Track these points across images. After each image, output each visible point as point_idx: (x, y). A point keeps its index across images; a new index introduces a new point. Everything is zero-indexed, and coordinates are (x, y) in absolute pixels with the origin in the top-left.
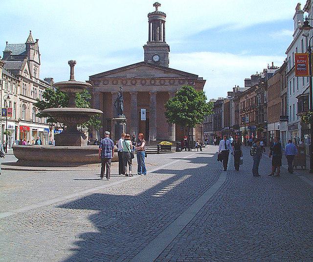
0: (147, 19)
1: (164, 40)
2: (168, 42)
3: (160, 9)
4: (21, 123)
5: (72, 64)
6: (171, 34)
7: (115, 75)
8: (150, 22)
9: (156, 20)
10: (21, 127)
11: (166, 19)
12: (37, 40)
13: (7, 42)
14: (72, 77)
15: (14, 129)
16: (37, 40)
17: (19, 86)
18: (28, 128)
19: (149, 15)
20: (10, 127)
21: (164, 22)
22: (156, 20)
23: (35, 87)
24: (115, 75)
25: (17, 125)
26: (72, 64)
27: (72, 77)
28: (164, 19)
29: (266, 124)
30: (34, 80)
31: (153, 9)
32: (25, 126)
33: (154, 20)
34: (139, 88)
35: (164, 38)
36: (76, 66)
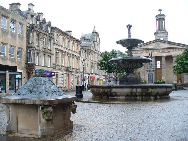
0: (155, 19)
1: (165, 29)
2: (167, 30)
3: (162, 13)
4: (91, 75)
5: (129, 27)
6: (168, 26)
8: (157, 20)
9: (161, 19)
10: (91, 77)
11: (166, 18)
12: (98, 31)
14: (130, 36)
15: (87, 78)
16: (98, 31)
18: (95, 77)
19: (157, 16)
20: (85, 77)
21: (164, 19)
22: (161, 19)
23: (98, 56)
25: (89, 76)
26: (129, 27)
27: (130, 36)
28: (164, 18)
30: (97, 52)
31: (158, 13)
32: (93, 77)
33: (160, 19)
35: (165, 28)
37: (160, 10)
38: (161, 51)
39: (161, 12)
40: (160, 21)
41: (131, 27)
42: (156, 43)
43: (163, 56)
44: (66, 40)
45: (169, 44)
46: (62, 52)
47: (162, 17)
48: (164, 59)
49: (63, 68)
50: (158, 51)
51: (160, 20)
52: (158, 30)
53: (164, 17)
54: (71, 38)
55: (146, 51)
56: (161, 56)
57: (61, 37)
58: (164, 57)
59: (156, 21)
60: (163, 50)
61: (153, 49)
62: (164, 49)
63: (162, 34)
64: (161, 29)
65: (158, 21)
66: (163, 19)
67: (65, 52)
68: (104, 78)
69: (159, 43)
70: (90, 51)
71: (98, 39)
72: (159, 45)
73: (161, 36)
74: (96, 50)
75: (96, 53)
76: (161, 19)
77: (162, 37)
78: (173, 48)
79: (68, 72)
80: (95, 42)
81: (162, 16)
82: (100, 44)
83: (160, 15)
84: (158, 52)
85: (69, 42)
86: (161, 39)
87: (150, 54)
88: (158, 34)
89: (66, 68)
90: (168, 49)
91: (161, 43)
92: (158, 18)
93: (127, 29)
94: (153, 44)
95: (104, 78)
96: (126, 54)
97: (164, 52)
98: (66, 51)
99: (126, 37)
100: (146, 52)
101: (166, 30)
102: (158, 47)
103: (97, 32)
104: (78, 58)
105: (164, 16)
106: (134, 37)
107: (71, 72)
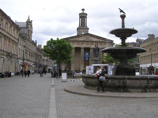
0: (79, 16)
1: (86, 26)
3: (85, 12)
4: (25, 61)
6: (89, 22)
7: (74, 39)
8: (80, 17)
9: (83, 17)
10: (25, 63)
11: (87, 16)
12: (32, 21)
13: (16, 21)
16: (32, 21)
17: (25, 42)
18: (27, 63)
19: (80, 14)
21: (86, 17)
22: (83, 17)
23: (30, 44)
24: (74, 39)
29: (139, 65)
30: (30, 39)
31: (82, 12)
32: (26, 63)
33: (83, 17)
34: (85, 45)
35: (86, 25)
37: (83, 10)
38: (90, 43)
40: (83, 19)
43: (91, 48)
44: (9, 25)
45: (97, 38)
46: (5, 37)
47: (85, 15)
48: (92, 51)
49: (5, 53)
50: (87, 43)
51: (83, 17)
54: (12, 24)
56: (80, 47)
57: (5, 21)
58: (92, 48)
60: (92, 43)
61: (84, 41)
62: (93, 42)
63: (84, 29)
64: (83, 25)
67: (8, 37)
68: (33, 64)
69: (88, 36)
70: (25, 38)
71: (31, 28)
73: (83, 31)
74: (29, 38)
75: (29, 41)
76: (84, 17)
77: (84, 32)
78: (100, 42)
79: (9, 57)
80: (29, 31)
82: (32, 33)
83: (83, 13)
84: (87, 44)
85: (11, 27)
86: (83, 33)
87: (96, 46)
88: (80, 29)
89: (7, 53)
90: (95, 42)
91: (90, 36)
92: (81, 16)
93: (121, 19)
94: (83, 37)
95: (33, 64)
96: (121, 44)
97: (92, 44)
98: (8, 35)
99: (120, 27)
100: (77, 43)
103: (31, 21)
104: (17, 44)
105: (86, 14)
106: (128, 26)
107: (11, 57)
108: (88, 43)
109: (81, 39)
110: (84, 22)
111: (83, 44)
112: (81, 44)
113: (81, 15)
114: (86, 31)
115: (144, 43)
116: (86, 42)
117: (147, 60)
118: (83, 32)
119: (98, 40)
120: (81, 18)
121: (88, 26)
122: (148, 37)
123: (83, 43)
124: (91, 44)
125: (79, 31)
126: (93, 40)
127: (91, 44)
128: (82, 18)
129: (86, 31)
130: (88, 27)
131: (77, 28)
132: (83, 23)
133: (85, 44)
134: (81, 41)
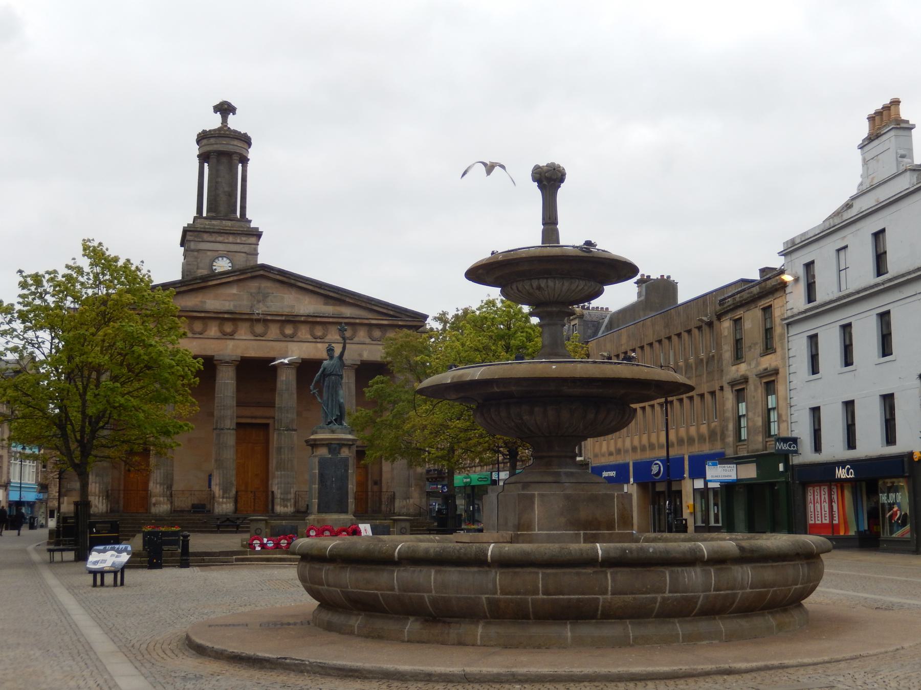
0: (195, 150)
3: (234, 123)
8: (204, 157)
11: (252, 154)
19: (203, 137)
21: (244, 160)
31: (214, 122)
33: (221, 154)
35: (243, 208)
36: (563, 193)
37: (225, 109)
39: (231, 117)
40: (223, 169)
41: (562, 180)
42: (254, 285)
50: (259, 328)
51: (224, 160)
52: (205, 214)
53: (246, 146)
55: (252, 327)
59: (196, 162)
60: (289, 330)
62: (291, 320)
63: (231, 239)
64: (223, 208)
65: (206, 165)
66: (235, 158)
69: (265, 284)
72: (265, 296)
76: (228, 155)
77: (227, 255)
81: (236, 142)
83: (224, 133)
86: (222, 265)
87: (330, 351)
88: (206, 237)
90: (312, 321)
91: (278, 285)
94: (234, 290)
97: (291, 338)
101: (249, 216)
102: (260, 309)
105: (246, 140)
108: (267, 327)
109: (212, 302)
110: (226, 189)
111: (231, 335)
112: (219, 334)
113: (212, 140)
114: (246, 249)
115: (610, 326)
116: (251, 320)
117: (636, 438)
118: (222, 257)
119: (329, 309)
120: (213, 160)
121: (256, 216)
122: (639, 294)
123: (228, 328)
124: (281, 337)
125: (198, 251)
126: (293, 307)
127: (285, 336)
128: (218, 161)
129: (246, 249)
130: (253, 225)
131: (186, 231)
132: (223, 198)
133: (243, 332)
134: (221, 318)
